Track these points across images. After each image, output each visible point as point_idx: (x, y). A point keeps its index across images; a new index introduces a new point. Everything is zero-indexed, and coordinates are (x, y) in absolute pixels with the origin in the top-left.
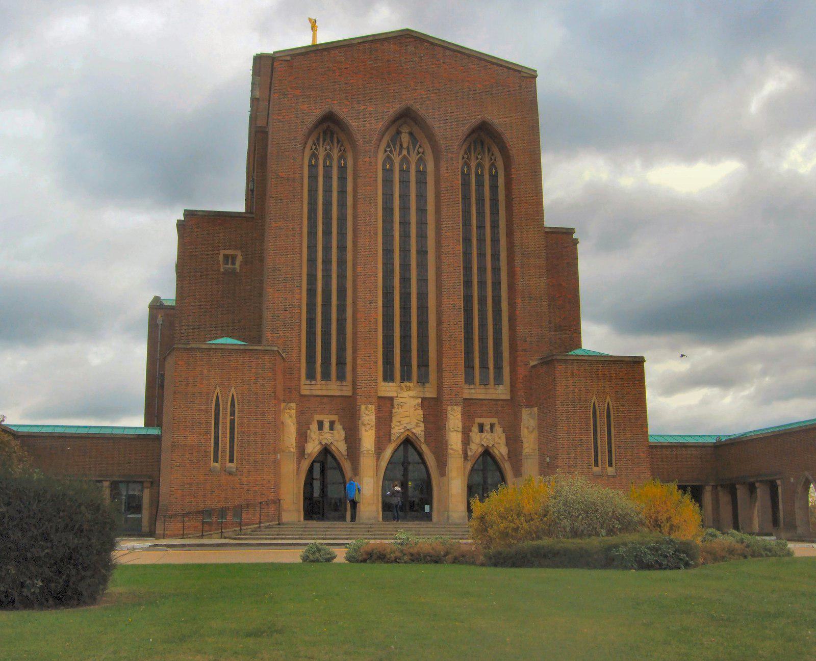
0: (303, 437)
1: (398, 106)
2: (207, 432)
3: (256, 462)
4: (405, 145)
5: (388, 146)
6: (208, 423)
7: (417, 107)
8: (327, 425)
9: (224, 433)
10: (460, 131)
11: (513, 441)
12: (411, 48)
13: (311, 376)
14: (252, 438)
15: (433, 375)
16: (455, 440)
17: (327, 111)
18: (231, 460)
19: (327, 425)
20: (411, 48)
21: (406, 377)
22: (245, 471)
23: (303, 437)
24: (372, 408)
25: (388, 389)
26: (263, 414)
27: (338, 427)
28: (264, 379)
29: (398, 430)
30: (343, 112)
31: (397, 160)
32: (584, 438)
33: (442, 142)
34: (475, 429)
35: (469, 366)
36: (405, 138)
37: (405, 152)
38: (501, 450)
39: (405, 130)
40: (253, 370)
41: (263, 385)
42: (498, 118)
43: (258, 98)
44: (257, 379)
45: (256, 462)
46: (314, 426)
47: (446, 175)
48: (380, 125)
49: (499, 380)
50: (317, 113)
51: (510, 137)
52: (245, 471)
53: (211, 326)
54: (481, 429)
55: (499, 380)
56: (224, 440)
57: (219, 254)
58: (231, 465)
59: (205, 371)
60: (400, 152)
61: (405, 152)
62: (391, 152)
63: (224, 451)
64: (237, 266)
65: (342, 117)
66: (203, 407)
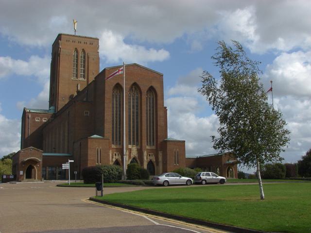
8: (117, 155)
11: (157, 158)
12: (136, 68)
15: (139, 143)
16: (145, 158)
19: (117, 155)
20: (136, 68)
21: (134, 144)
25: (130, 147)
27: (120, 155)
29: (132, 156)
34: (148, 155)
35: (147, 142)
36: (134, 89)
38: (154, 160)
39: (134, 87)
42: (156, 86)
49: (154, 145)
51: (158, 90)
54: (150, 156)
55: (154, 145)
64: (88, 115)
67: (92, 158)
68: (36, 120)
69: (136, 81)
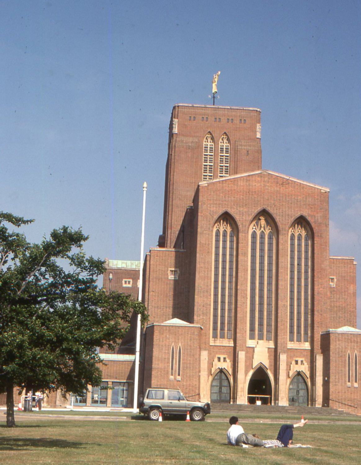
0: (211, 365)
1: (259, 209)
2: (168, 363)
3: (190, 376)
4: (262, 226)
5: (254, 226)
6: (169, 359)
7: (269, 209)
9: (176, 363)
10: (290, 220)
12: (266, 179)
13: (215, 336)
14: (188, 365)
17: (225, 211)
18: (179, 375)
22: (185, 380)
23: (211, 365)
24: (243, 353)
25: (250, 343)
26: (193, 355)
28: (194, 339)
30: (232, 212)
31: (258, 233)
32: (343, 369)
33: (280, 226)
37: (262, 229)
40: (189, 336)
41: (194, 342)
43: (177, 134)
44: (191, 339)
45: (190, 376)
46: (216, 360)
47: (282, 242)
48: (251, 218)
50: (221, 212)
52: (185, 380)
53: (163, 307)
56: (176, 367)
57: (168, 270)
58: (179, 377)
59: (168, 336)
60: (260, 229)
61: (262, 229)
62: (255, 229)
63: (175, 371)
65: (231, 214)
66: (167, 352)
67: (161, 365)
68: (124, 285)
69: (265, 207)
